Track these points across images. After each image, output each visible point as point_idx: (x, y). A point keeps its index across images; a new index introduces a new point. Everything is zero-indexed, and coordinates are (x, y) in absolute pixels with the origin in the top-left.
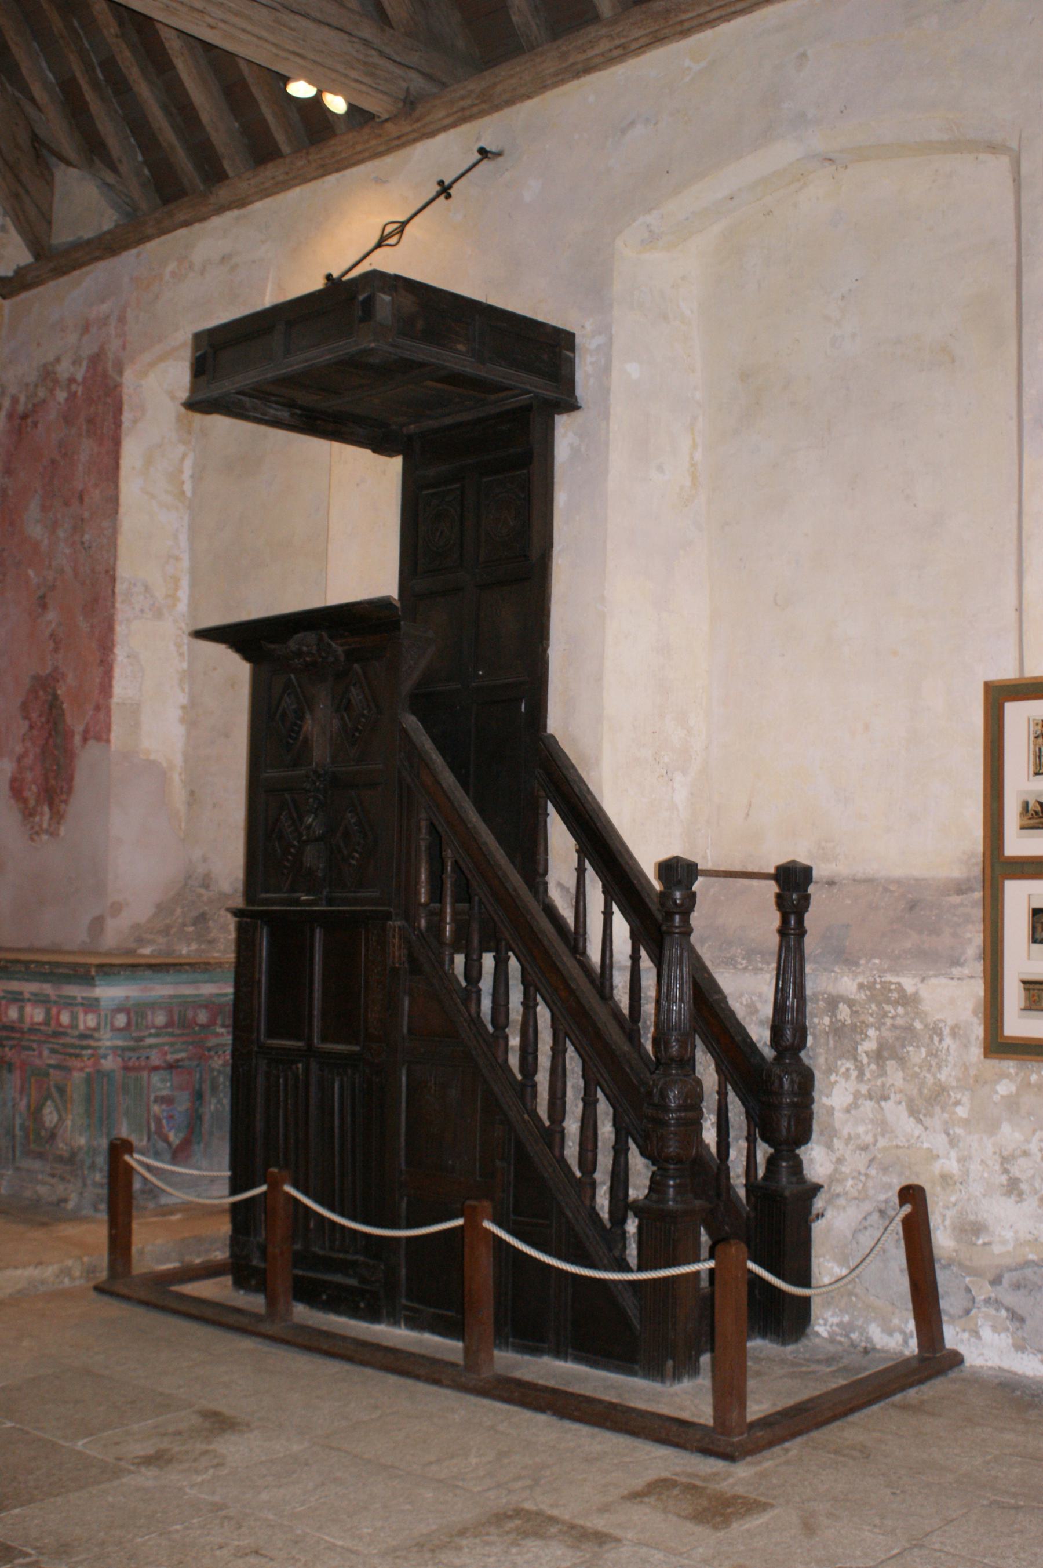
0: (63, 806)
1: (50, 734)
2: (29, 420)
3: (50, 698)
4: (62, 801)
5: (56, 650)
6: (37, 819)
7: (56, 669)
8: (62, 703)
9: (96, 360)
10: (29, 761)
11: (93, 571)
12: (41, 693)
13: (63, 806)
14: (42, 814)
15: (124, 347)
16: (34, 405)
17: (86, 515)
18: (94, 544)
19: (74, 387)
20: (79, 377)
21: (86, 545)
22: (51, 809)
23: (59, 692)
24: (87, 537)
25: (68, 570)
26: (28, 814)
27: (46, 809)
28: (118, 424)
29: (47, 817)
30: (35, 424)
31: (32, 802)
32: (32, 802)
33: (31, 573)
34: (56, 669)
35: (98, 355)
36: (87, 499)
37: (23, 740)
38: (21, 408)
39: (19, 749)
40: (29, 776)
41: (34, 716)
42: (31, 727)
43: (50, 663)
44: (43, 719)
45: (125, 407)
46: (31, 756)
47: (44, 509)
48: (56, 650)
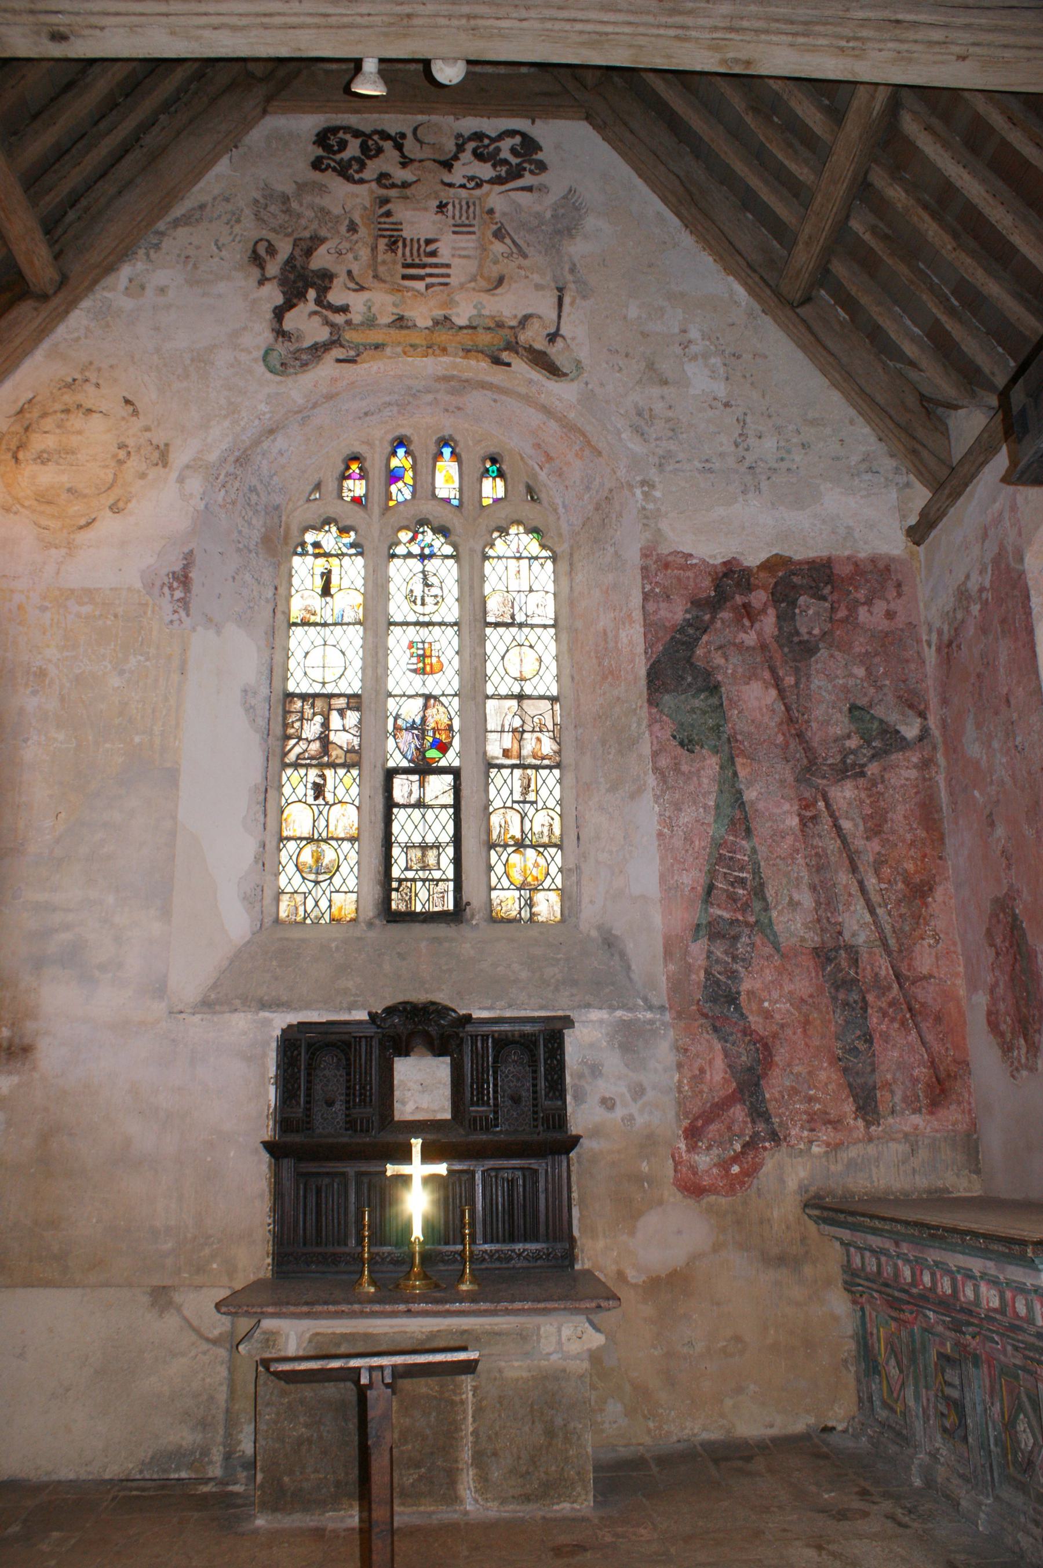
0: (1037, 1036)
1: (1015, 958)
2: (954, 645)
3: (1009, 919)
4: (1035, 1032)
5: (1009, 867)
6: (1016, 1053)
7: (1011, 886)
8: (1022, 922)
9: (997, 560)
10: (1000, 990)
11: (1029, 773)
12: (1001, 916)
13: (1037, 1036)
14: (1019, 1048)
15: (1020, 534)
16: (956, 630)
17: (1015, 716)
18: (1026, 744)
19: (984, 595)
20: (987, 585)
21: (1019, 749)
22: (1026, 1041)
23: (1017, 911)
24: (1019, 739)
25: (1007, 779)
26: (1007, 1049)
27: (1022, 1041)
28: (1028, 613)
29: (1023, 1051)
30: (959, 647)
31: (1008, 1036)
32: (1008, 1036)
33: (976, 793)
34: (1011, 886)
35: (999, 554)
36: (1013, 701)
37: (993, 970)
38: (946, 637)
39: (989, 979)
40: (1002, 1007)
41: (998, 941)
42: (998, 954)
43: (1005, 881)
44: (1007, 944)
45: (1032, 592)
46: (1001, 984)
47: (979, 726)
48: (1009, 867)
